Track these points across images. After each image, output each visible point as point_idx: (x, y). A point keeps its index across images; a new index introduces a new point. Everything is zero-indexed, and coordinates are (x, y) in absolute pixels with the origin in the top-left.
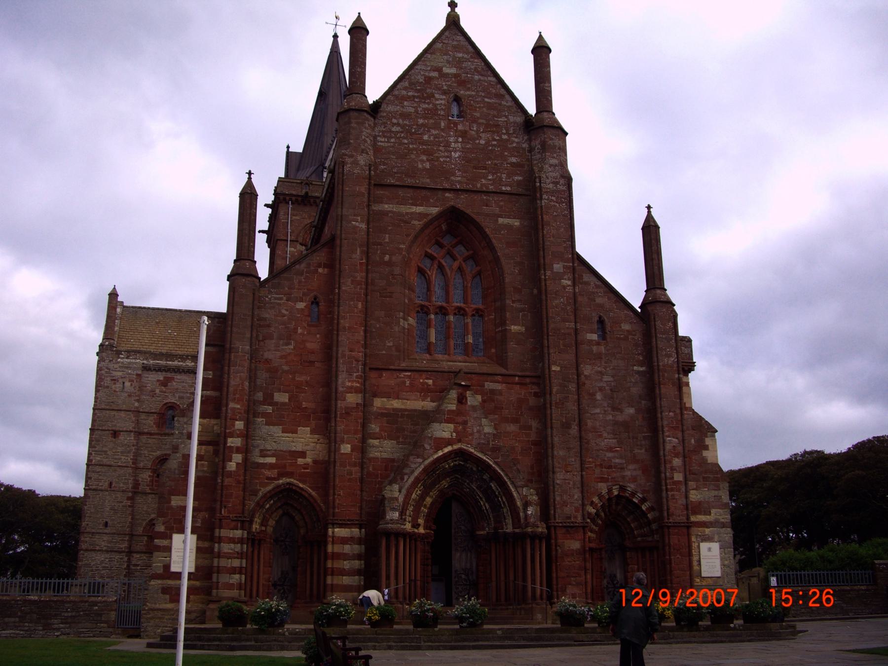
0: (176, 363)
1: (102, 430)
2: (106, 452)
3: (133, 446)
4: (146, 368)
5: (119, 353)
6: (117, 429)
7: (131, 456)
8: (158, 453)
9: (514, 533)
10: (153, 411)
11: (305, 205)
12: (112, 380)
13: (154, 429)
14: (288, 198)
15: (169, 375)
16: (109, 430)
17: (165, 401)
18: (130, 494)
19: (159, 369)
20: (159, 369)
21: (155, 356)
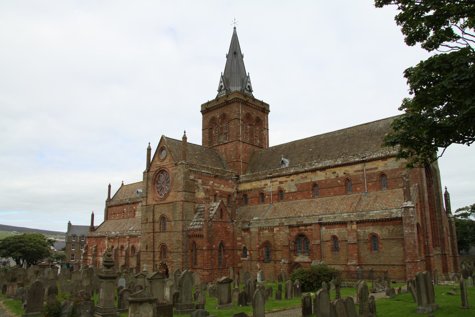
11: (244, 105)
14: (240, 100)
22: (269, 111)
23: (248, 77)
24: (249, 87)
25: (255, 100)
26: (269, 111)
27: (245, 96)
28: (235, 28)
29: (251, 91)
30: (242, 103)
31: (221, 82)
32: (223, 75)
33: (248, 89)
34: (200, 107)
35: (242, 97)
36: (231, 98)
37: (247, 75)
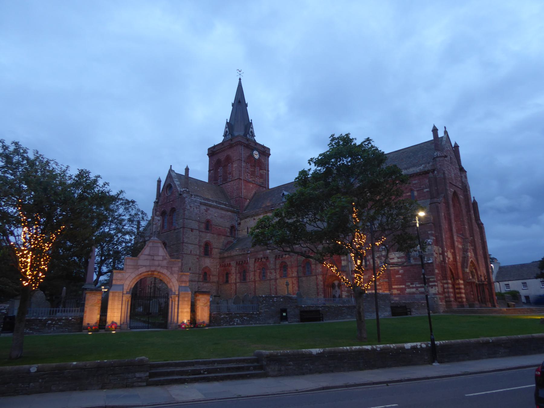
0: (210, 203)
1: (188, 228)
2: (189, 237)
3: (198, 236)
4: (201, 203)
5: (192, 195)
6: (192, 228)
7: (198, 240)
8: (205, 240)
9: (479, 284)
10: (203, 222)
12: (190, 207)
13: (204, 230)
15: (208, 207)
16: (190, 228)
17: (207, 218)
18: (198, 257)
19: (205, 204)
20: (205, 204)
21: (204, 199)
22: (270, 154)
23: (251, 123)
24: (251, 132)
25: (256, 144)
26: (270, 154)
27: (248, 140)
28: (240, 79)
29: (253, 135)
30: (244, 146)
31: (226, 128)
32: (228, 121)
33: (251, 134)
34: (207, 151)
35: (244, 141)
36: (234, 141)
37: (250, 122)
